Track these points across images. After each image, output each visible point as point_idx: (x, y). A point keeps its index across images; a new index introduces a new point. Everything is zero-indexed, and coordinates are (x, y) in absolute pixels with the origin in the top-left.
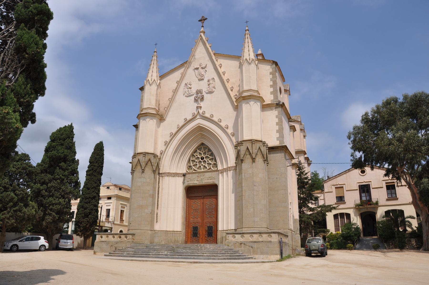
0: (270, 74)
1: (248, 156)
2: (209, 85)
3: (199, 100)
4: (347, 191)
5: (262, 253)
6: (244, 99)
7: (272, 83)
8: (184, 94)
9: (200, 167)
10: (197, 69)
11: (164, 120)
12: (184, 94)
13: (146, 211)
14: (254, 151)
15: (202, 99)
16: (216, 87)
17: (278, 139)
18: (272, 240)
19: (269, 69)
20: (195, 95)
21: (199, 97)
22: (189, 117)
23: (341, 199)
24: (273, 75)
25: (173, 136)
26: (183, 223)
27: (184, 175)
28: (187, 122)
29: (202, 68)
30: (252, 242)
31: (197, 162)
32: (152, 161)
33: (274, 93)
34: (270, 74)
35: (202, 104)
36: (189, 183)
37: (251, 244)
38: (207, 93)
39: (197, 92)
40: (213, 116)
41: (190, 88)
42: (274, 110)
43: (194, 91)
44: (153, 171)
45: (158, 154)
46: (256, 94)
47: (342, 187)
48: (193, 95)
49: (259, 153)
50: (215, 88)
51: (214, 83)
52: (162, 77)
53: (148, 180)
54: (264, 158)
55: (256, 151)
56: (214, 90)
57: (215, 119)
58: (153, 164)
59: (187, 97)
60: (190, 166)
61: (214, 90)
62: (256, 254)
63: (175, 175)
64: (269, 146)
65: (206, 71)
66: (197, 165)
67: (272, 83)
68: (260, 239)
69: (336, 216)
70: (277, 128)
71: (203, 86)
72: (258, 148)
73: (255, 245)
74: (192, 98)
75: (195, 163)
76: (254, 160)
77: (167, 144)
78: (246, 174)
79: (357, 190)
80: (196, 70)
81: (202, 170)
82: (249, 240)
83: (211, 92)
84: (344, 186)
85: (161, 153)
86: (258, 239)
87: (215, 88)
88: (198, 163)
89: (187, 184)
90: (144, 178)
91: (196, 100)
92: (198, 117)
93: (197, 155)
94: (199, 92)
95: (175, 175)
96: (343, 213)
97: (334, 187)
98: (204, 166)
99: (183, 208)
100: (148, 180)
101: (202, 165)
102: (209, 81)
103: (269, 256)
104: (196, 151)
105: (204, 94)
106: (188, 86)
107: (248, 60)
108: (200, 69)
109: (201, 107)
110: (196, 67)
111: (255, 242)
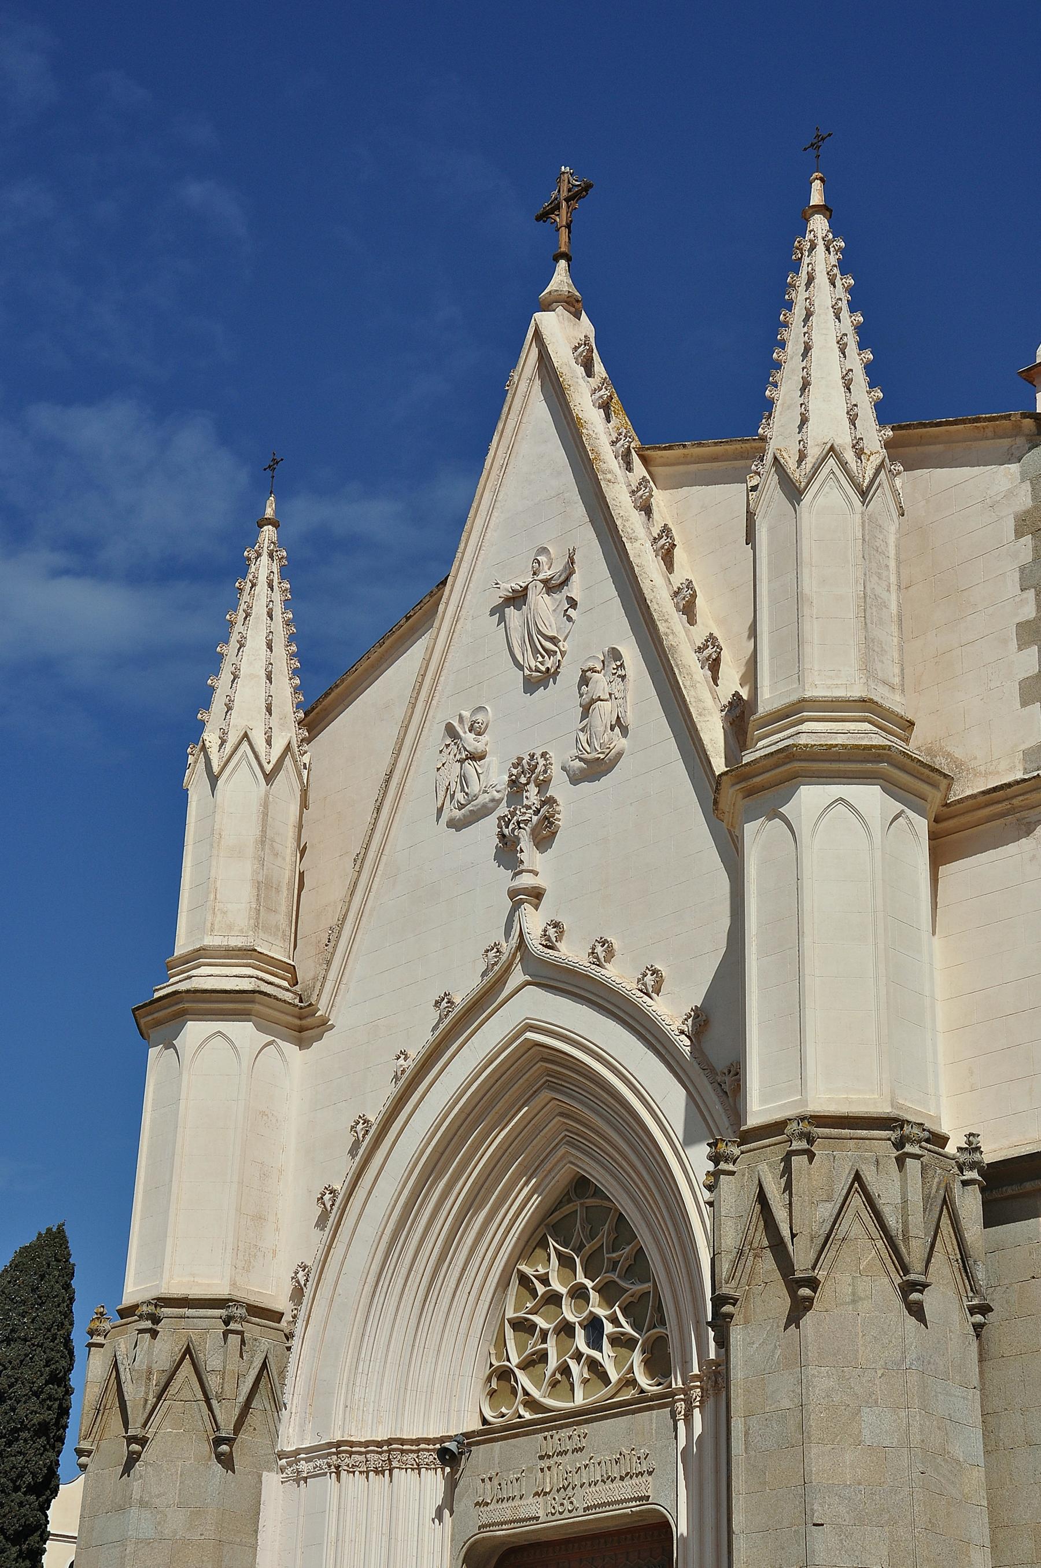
0: (1019, 534)
1: (768, 1263)
2: (586, 710)
3: (526, 843)
6: (750, 793)
7: (1029, 611)
8: (440, 810)
10: (518, 598)
11: (324, 1025)
12: (440, 810)
14: (806, 1216)
15: (545, 835)
16: (630, 719)
19: (1009, 494)
20: (503, 810)
21: (524, 822)
24: (1037, 532)
25: (371, 1140)
27: (450, 1456)
28: (459, 1022)
29: (551, 587)
31: (544, 1334)
32: (212, 1359)
34: (1019, 534)
35: (539, 866)
36: (487, 1515)
38: (575, 779)
39: (513, 782)
40: (610, 953)
41: (475, 757)
43: (494, 776)
44: (218, 1441)
45: (282, 1303)
46: (859, 732)
48: (497, 802)
49: (857, 1225)
50: (625, 731)
51: (617, 686)
53: (176, 1522)
54: (906, 1270)
55: (826, 1211)
56: (620, 743)
58: (213, 1382)
59: (455, 825)
60: (505, 1374)
61: (620, 743)
63: (387, 1455)
64: (992, 1152)
65: (573, 603)
66: (543, 1357)
71: (550, 727)
72: (844, 1179)
74: (487, 830)
75: (533, 1345)
76: (801, 1294)
77: (332, 1212)
78: (753, 1422)
80: (510, 612)
81: (580, 1399)
83: (594, 769)
85: (298, 1294)
87: (625, 731)
88: (551, 1346)
90: (143, 1504)
91: (507, 851)
92: (517, 976)
93: (545, 1280)
95: (387, 1455)
98: (594, 1366)
100: (176, 1522)
101: (578, 1356)
102: (584, 681)
104: (543, 1244)
105: (560, 788)
106: (462, 748)
107: (849, 456)
108: (542, 603)
109: (537, 895)
110: (508, 586)
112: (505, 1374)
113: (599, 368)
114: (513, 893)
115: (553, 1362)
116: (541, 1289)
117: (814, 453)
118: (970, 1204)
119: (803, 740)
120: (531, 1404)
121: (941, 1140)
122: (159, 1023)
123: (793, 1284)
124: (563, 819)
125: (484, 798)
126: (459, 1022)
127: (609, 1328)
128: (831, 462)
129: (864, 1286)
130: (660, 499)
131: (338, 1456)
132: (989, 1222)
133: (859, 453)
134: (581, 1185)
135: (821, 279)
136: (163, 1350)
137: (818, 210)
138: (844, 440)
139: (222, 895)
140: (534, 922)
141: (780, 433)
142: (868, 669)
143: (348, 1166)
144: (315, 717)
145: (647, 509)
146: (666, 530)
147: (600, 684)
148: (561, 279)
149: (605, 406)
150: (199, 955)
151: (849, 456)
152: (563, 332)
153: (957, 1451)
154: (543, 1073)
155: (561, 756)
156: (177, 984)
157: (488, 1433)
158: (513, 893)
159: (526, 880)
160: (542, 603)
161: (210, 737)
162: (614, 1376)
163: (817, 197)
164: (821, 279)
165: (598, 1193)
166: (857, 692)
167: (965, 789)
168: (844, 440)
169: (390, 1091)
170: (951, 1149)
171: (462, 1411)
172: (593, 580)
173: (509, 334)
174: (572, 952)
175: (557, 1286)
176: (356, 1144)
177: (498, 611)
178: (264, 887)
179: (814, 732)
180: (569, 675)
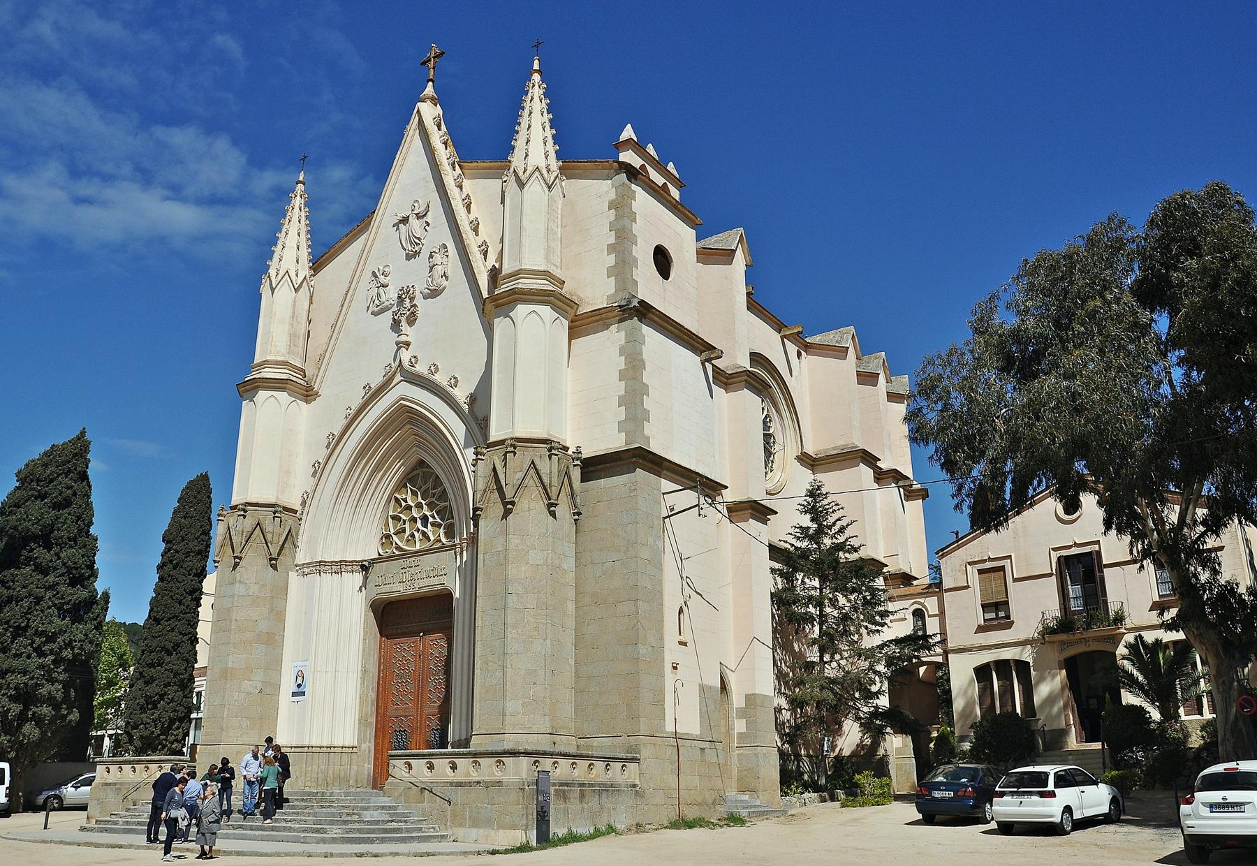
1: (496, 495)
3: (404, 322)
4: (1015, 580)
5: (476, 823)
6: (497, 306)
7: (612, 240)
9: (413, 535)
10: (405, 221)
11: (317, 394)
13: (247, 685)
14: (511, 478)
15: (412, 320)
16: (449, 274)
17: (622, 426)
18: (505, 779)
19: (607, 192)
20: (395, 308)
21: (403, 313)
22: (376, 382)
23: (997, 612)
25: (335, 443)
26: (363, 722)
27: (365, 568)
28: (374, 395)
29: (419, 217)
30: (451, 784)
32: (268, 527)
33: (622, 268)
36: (379, 590)
37: (449, 792)
40: (437, 370)
42: (614, 327)
43: (391, 294)
44: (271, 559)
45: (297, 507)
47: (1002, 569)
49: (531, 481)
50: (447, 279)
52: (317, 265)
53: (254, 589)
55: (520, 475)
56: (445, 283)
57: (441, 379)
58: (269, 537)
59: (375, 314)
60: (388, 537)
61: (445, 283)
62: (461, 825)
63: (339, 566)
64: (584, 456)
65: (428, 224)
66: (404, 530)
67: (612, 240)
68: (475, 775)
69: (982, 673)
70: (620, 388)
71: (415, 275)
73: (459, 796)
74: (387, 318)
75: (400, 525)
76: (508, 507)
77: (318, 471)
79: (1050, 575)
80: (401, 226)
81: (418, 547)
82: (445, 779)
83: (434, 293)
84: (1007, 563)
85: (304, 503)
86: (468, 774)
87: (447, 279)
88: (407, 526)
89: (373, 592)
90: (240, 582)
92: (398, 378)
93: (405, 501)
94: (405, 295)
95: (339, 566)
96: (1005, 663)
97: (972, 571)
98: (424, 534)
99: (364, 671)
100: (254, 589)
101: (418, 530)
102: (431, 256)
103: (492, 832)
105: (419, 300)
107: (544, 171)
108: (414, 222)
109: (408, 344)
110: (401, 215)
111: (460, 784)
112: (388, 537)
113: (443, 127)
114: (397, 343)
115: (408, 533)
116: (404, 504)
117: (530, 170)
118: (576, 474)
119: (520, 286)
120: (398, 548)
121: (566, 449)
122: (247, 391)
123: (505, 504)
124: (420, 314)
125: (387, 303)
126: (374, 395)
127: (431, 520)
128: (537, 173)
129: (533, 504)
130: (467, 183)
131: (320, 566)
132: (584, 479)
133: (548, 171)
134: (421, 463)
135: (536, 99)
136: (249, 523)
137: (536, 71)
138: (542, 165)
139: (275, 339)
140: (406, 355)
141: (517, 160)
142: (547, 259)
143: (326, 452)
144: (317, 265)
145: (461, 187)
146: (468, 196)
147: (438, 258)
148: (429, 90)
149: (445, 143)
150: (265, 363)
151: (544, 171)
152: (429, 111)
153: (565, 566)
154: (406, 416)
155: (420, 287)
156: (255, 375)
157: (381, 559)
158: (397, 343)
159: (403, 338)
160: (414, 222)
161: (272, 272)
162: (432, 538)
163: (536, 67)
164: (536, 99)
165: (428, 466)
166: (542, 269)
167: (582, 310)
168: (542, 165)
169: (344, 422)
170: (570, 452)
171: (371, 550)
172: (437, 215)
173: (406, 111)
174: (421, 369)
175: (410, 502)
176: (329, 444)
177: (396, 225)
178: (293, 336)
179: (524, 283)
180: (425, 254)
